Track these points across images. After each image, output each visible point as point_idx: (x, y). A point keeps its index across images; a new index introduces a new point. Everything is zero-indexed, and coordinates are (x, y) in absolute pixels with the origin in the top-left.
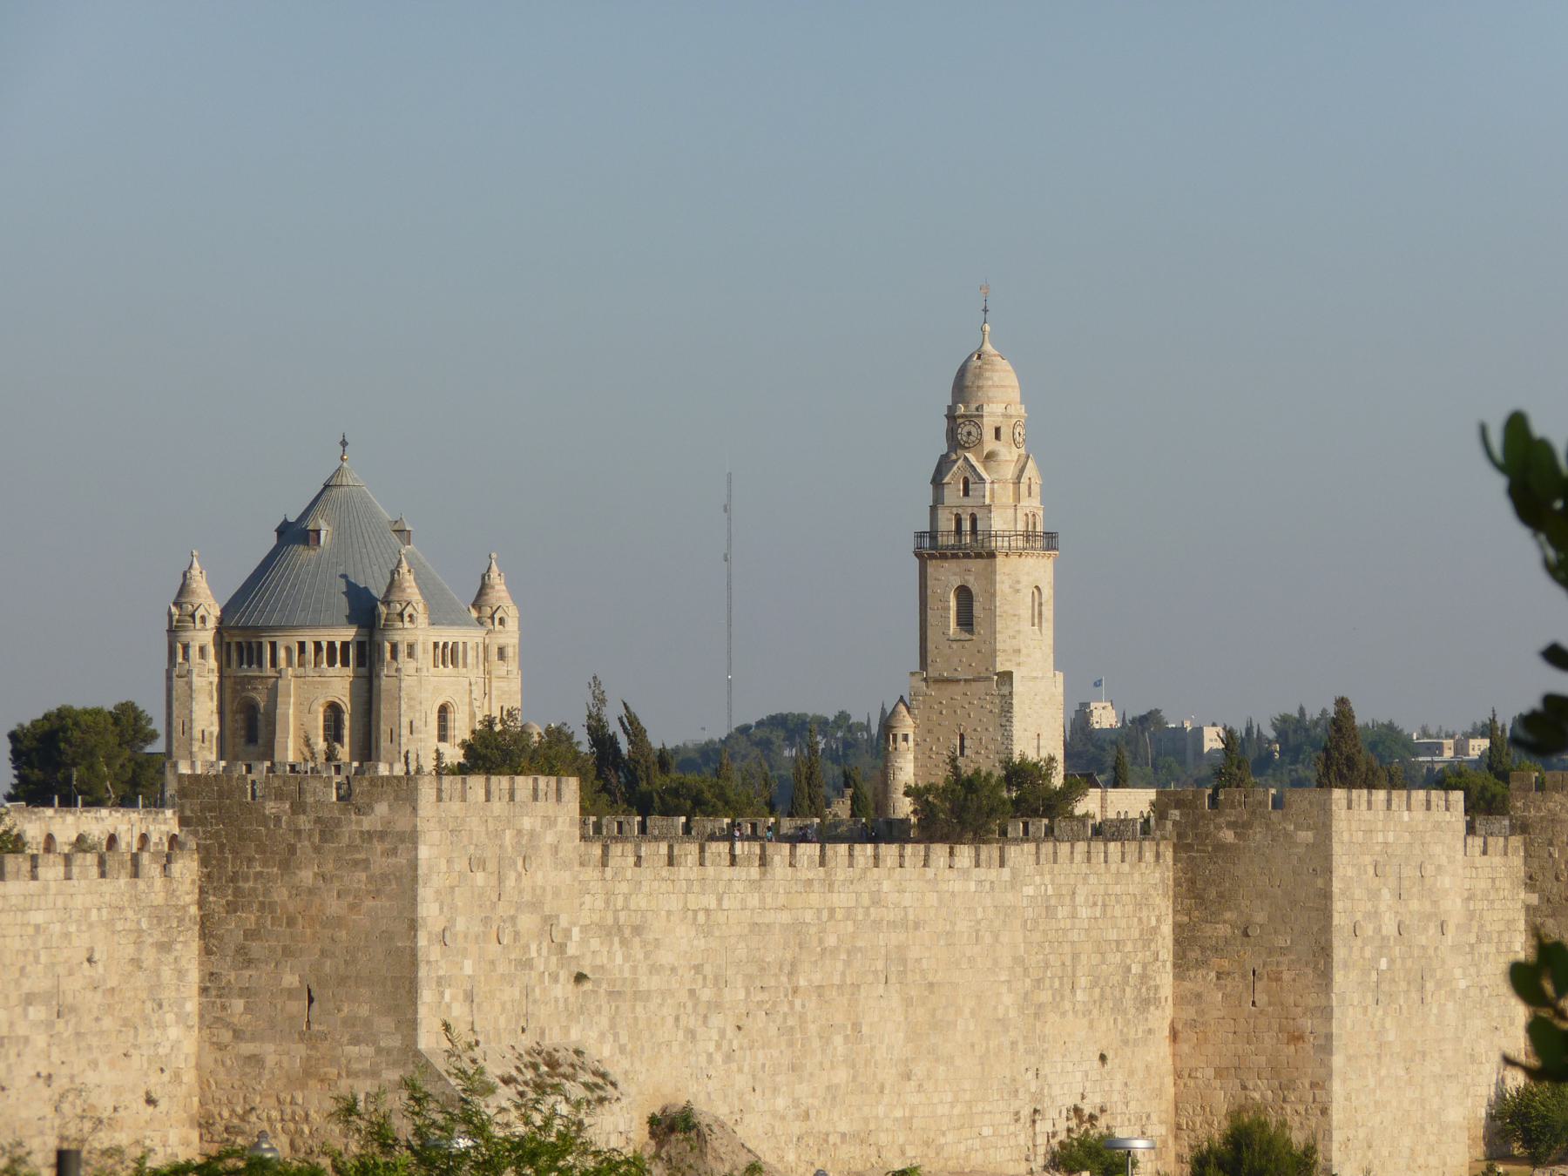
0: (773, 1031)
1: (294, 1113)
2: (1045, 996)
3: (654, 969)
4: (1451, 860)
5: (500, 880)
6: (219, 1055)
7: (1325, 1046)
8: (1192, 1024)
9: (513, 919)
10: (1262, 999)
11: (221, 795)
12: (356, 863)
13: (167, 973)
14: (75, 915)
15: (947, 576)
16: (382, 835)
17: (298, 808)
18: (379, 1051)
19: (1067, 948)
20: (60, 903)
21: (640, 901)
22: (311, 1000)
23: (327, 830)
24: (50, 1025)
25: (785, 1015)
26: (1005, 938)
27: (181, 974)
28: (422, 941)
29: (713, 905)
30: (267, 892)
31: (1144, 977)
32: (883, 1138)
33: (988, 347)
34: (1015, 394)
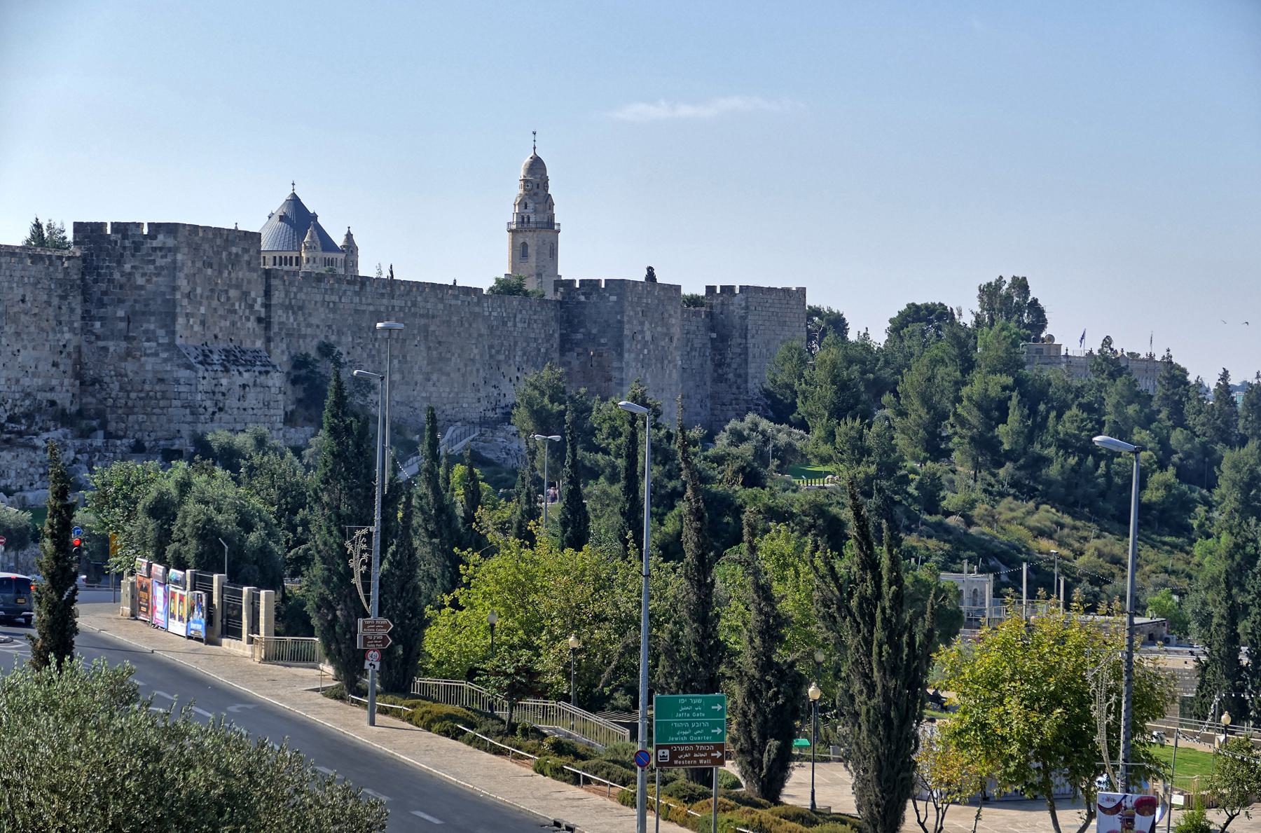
0: (365, 355)
2: (502, 357)
3: (309, 325)
4: (675, 312)
5: (220, 273)
9: (227, 292)
14: (16, 279)
16: (161, 249)
17: (125, 237)
18: (159, 344)
19: (511, 338)
20: (8, 273)
21: (301, 296)
23: (137, 247)
25: (371, 350)
26: (474, 325)
27: (72, 310)
29: (337, 300)
30: (111, 274)
32: (417, 405)
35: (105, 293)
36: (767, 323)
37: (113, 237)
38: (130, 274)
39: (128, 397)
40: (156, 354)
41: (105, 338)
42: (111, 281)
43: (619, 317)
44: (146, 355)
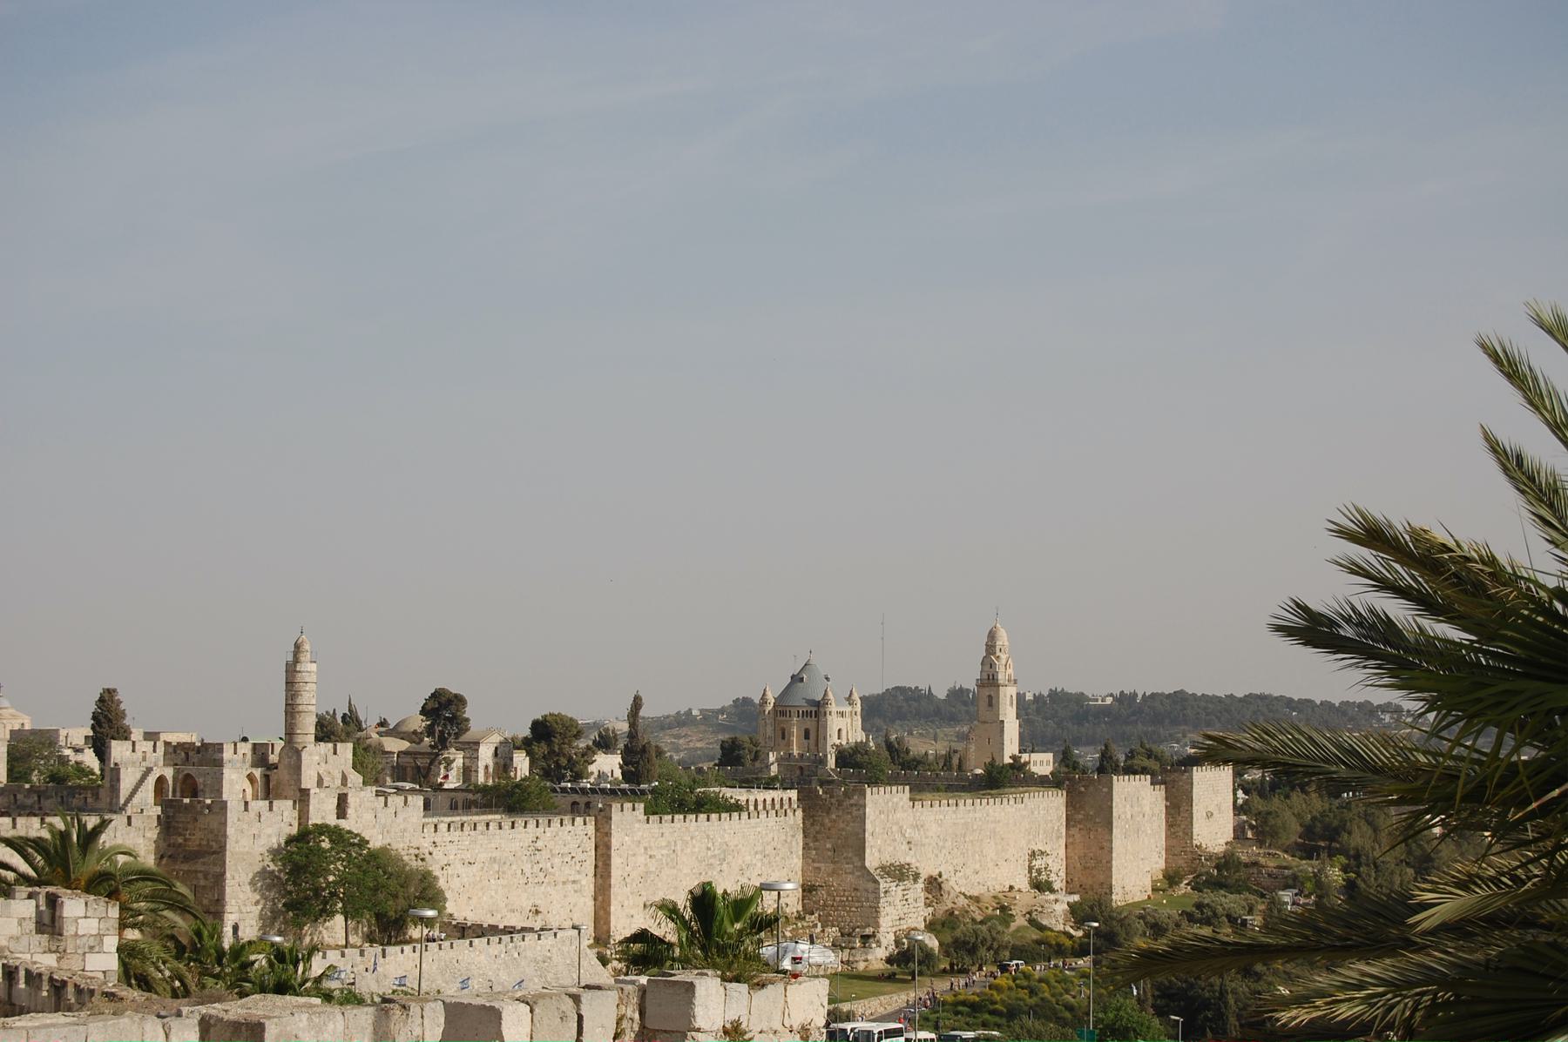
5: (888, 816)
8: (1072, 843)
10: (1092, 837)
12: (848, 813)
13: (794, 843)
15: (986, 692)
16: (856, 805)
18: (854, 867)
23: (840, 804)
28: (867, 835)
29: (943, 818)
31: (1058, 830)
32: (989, 883)
33: (998, 625)
34: (1006, 639)
35: (817, 833)
36: (1206, 793)
37: (824, 796)
38: (835, 821)
39: (834, 900)
40: (852, 873)
42: (822, 825)
44: (846, 873)
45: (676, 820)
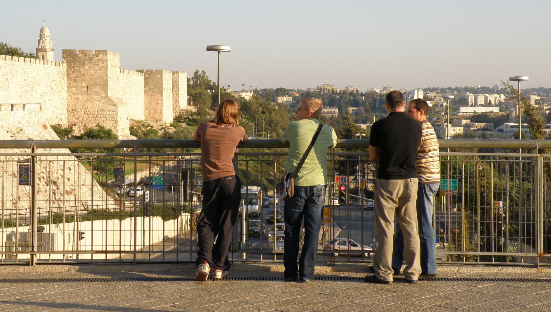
1: (85, 107)
6: (71, 97)
7: (162, 105)
11: (71, 53)
16: (101, 60)
17: (85, 55)
18: (101, 97)
22: (88, 88)
23: (91, 59)
24: (50, 91)
30: (80, 70)
33: (45, 26)
34: (49, 32)
35: (76, 77)
38: (88, 70)
40: (100, 100)
41: (78, 94)
43: (161, 83)
45: (7, 59)
